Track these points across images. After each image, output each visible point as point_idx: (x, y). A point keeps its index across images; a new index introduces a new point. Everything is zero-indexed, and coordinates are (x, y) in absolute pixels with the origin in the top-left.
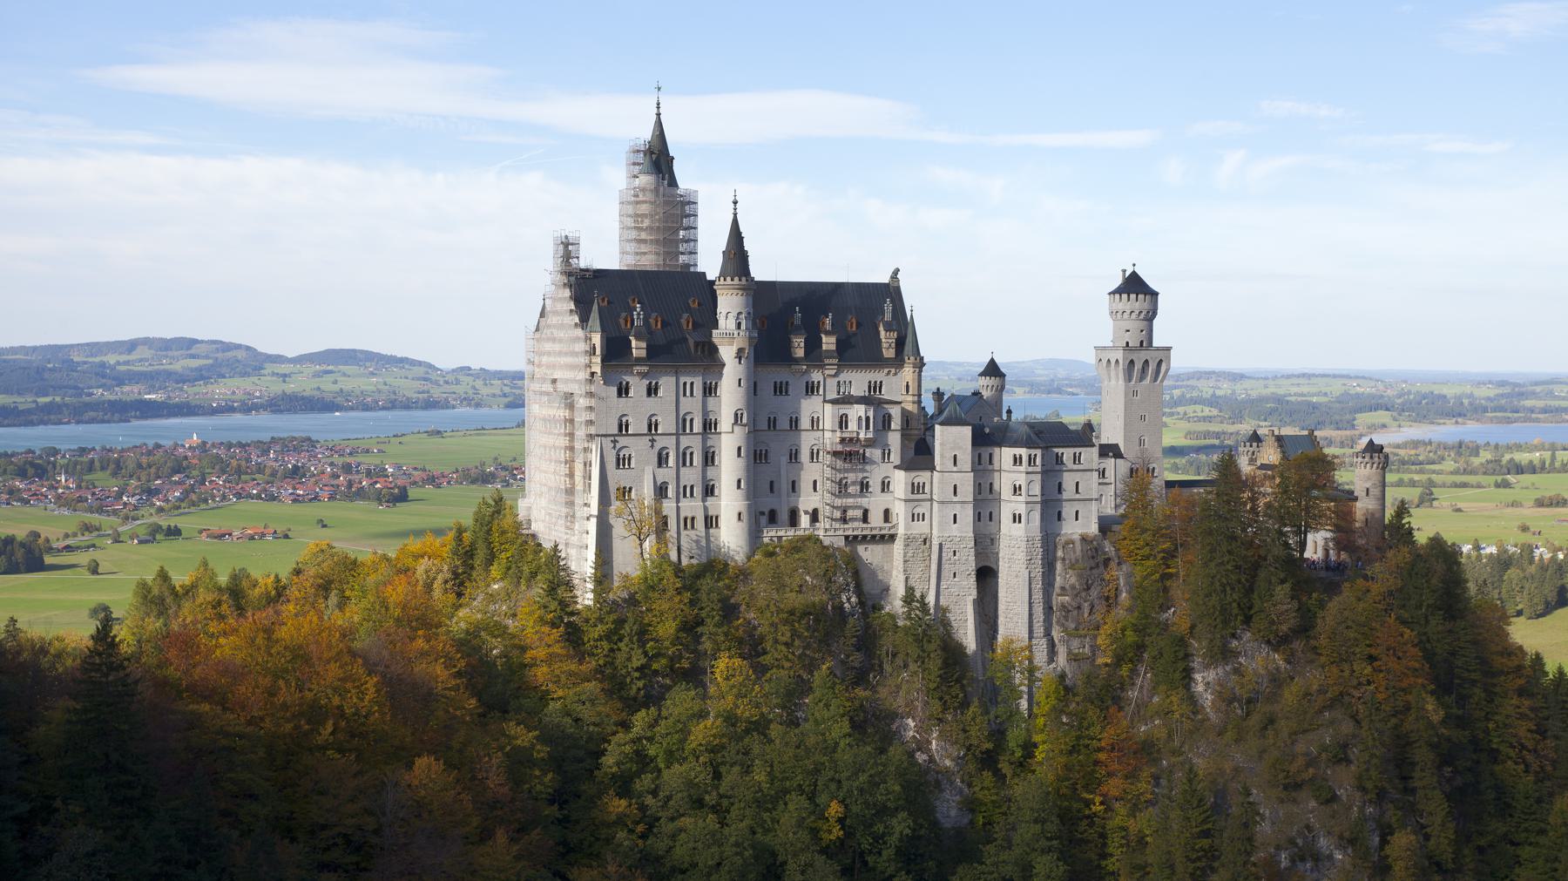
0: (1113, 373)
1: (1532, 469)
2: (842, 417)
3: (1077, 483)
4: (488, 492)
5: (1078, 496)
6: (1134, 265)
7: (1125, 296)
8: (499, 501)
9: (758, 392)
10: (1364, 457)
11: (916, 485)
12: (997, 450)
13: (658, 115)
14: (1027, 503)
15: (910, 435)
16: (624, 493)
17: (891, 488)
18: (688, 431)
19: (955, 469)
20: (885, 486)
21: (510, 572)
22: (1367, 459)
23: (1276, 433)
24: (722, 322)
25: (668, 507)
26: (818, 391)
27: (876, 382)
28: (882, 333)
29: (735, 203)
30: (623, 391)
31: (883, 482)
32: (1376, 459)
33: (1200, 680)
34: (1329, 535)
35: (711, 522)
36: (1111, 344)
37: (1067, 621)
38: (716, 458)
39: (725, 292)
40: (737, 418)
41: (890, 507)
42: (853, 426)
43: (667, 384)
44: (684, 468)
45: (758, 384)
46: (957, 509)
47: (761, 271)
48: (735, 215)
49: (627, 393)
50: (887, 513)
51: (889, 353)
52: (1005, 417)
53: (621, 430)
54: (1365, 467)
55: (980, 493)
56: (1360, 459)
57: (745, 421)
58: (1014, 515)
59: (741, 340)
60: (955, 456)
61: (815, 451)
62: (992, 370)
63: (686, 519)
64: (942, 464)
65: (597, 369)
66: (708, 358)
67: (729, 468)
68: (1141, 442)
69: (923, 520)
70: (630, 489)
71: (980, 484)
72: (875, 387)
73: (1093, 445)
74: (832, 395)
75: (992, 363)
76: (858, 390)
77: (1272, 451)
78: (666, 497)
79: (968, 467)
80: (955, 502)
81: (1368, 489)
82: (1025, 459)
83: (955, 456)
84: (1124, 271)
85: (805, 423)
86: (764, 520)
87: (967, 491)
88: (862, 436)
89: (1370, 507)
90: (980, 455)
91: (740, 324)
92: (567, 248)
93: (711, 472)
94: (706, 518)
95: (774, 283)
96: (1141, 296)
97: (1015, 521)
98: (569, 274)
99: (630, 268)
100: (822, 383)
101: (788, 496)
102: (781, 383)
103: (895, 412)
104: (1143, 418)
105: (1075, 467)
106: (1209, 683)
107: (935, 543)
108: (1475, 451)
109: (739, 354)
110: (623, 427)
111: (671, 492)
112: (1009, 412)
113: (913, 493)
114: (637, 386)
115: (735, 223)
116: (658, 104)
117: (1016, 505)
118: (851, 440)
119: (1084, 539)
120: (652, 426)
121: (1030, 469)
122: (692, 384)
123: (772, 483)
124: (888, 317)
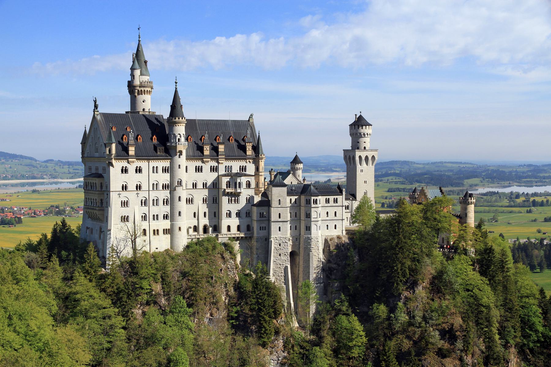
0: (352, 161)
1: (542, 204)
3: (336, 212)
4: (58, 220)
5: (336, 218)
6: (361, 112)
7: (357, 126)
8: (64, 223)
9: (188, 171)
12: (296, 197)
13: (139, 41)
16: (124, 218)
17: (250, 215)
18: (155, 189)
19: (279, 206)
25: (145, 225)
27: (243, 166)
31: (247, 212)
33: (391, 301)
37: (331, 275)
41: (250, 224)
45: (188, 167)
46: (280, 224)
48: (176, 88)
51: (250, 152)
53: (123, 189)
58: (307, 227)
60: (280, 200)
61: (215, 198)
62: (296, 160)
63: (154, 231)
68: (365, 193)
69: (265, 230)
72: (243, 169)
73: (342, 195)
75: (296, 156)
76: (236, 170)
77: (424, 197)
83: (280, 200)
84: (356, 115)
86: (191, 231)
90: (291, 199)
91: (179, 139)
94: (164, 230)
95: (195, 120)
102: (199, 166)
104: (365, 182)
107: (272, 239)
108: (518, 196)
110: (125, 188)
113: (260, 217)
114: (132, 168)
115: (176, 92)
116: (139, 36)
120: (139, 187)
122: (157, 167)
123: (195, 213)
124: (249, 136)
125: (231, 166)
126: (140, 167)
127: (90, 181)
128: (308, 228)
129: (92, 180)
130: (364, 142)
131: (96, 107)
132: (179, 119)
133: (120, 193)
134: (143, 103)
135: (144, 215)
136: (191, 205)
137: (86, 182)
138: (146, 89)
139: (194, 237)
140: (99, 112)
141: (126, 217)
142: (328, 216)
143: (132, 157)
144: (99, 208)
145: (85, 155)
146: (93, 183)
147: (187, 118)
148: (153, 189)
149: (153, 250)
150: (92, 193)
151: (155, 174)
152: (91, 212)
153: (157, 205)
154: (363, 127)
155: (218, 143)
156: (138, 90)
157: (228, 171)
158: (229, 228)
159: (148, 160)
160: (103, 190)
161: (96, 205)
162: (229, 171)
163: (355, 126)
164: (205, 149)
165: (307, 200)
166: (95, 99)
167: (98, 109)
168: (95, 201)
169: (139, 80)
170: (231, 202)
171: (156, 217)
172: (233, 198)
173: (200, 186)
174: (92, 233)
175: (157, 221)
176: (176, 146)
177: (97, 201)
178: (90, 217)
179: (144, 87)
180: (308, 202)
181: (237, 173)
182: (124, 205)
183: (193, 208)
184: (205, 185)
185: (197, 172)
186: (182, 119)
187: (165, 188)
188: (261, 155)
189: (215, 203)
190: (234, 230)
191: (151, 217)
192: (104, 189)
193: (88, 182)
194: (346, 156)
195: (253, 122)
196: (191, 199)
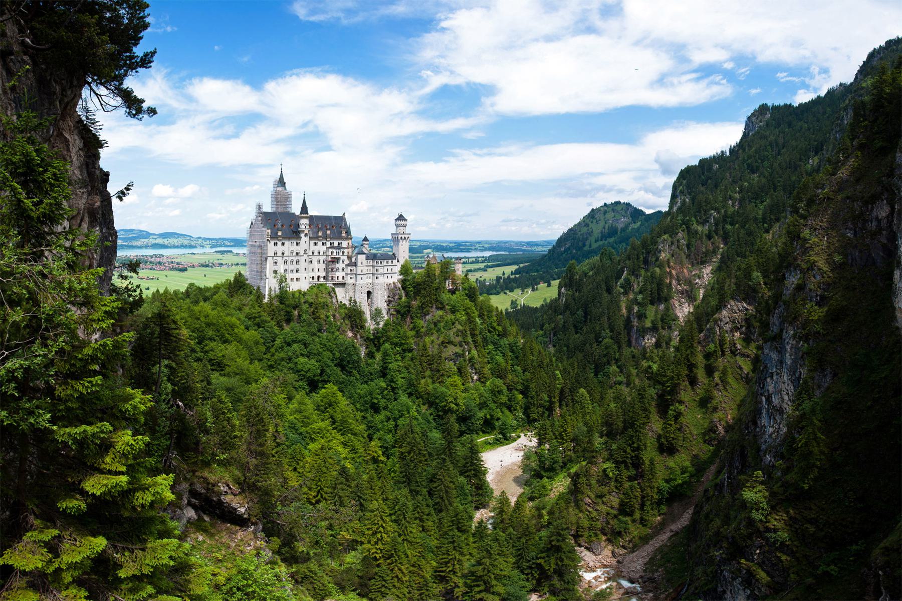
8: (240, 274)
30: (275, 244)
40: (305, 251)
42: (335, 254)
43: (287, 243)
47: (311, 212)
51: (344, 235)
59: (306, 231)
62: (366, 239)
72: (340, 244)
75: (366, 237)
76: (336, 244)
85: (322, 253)
92: (259, 207)
93: (298, 266)
109: (306, 235)
110: (275, 254)
114: (279, 243)
119: (394, 283)
120: (283, 254)
128: (377, 278)
149: (291, 290)
159: (289, 239)
171: (292, 271)
173: (316, 253)
180: (377, 263)
184: (319, 253)
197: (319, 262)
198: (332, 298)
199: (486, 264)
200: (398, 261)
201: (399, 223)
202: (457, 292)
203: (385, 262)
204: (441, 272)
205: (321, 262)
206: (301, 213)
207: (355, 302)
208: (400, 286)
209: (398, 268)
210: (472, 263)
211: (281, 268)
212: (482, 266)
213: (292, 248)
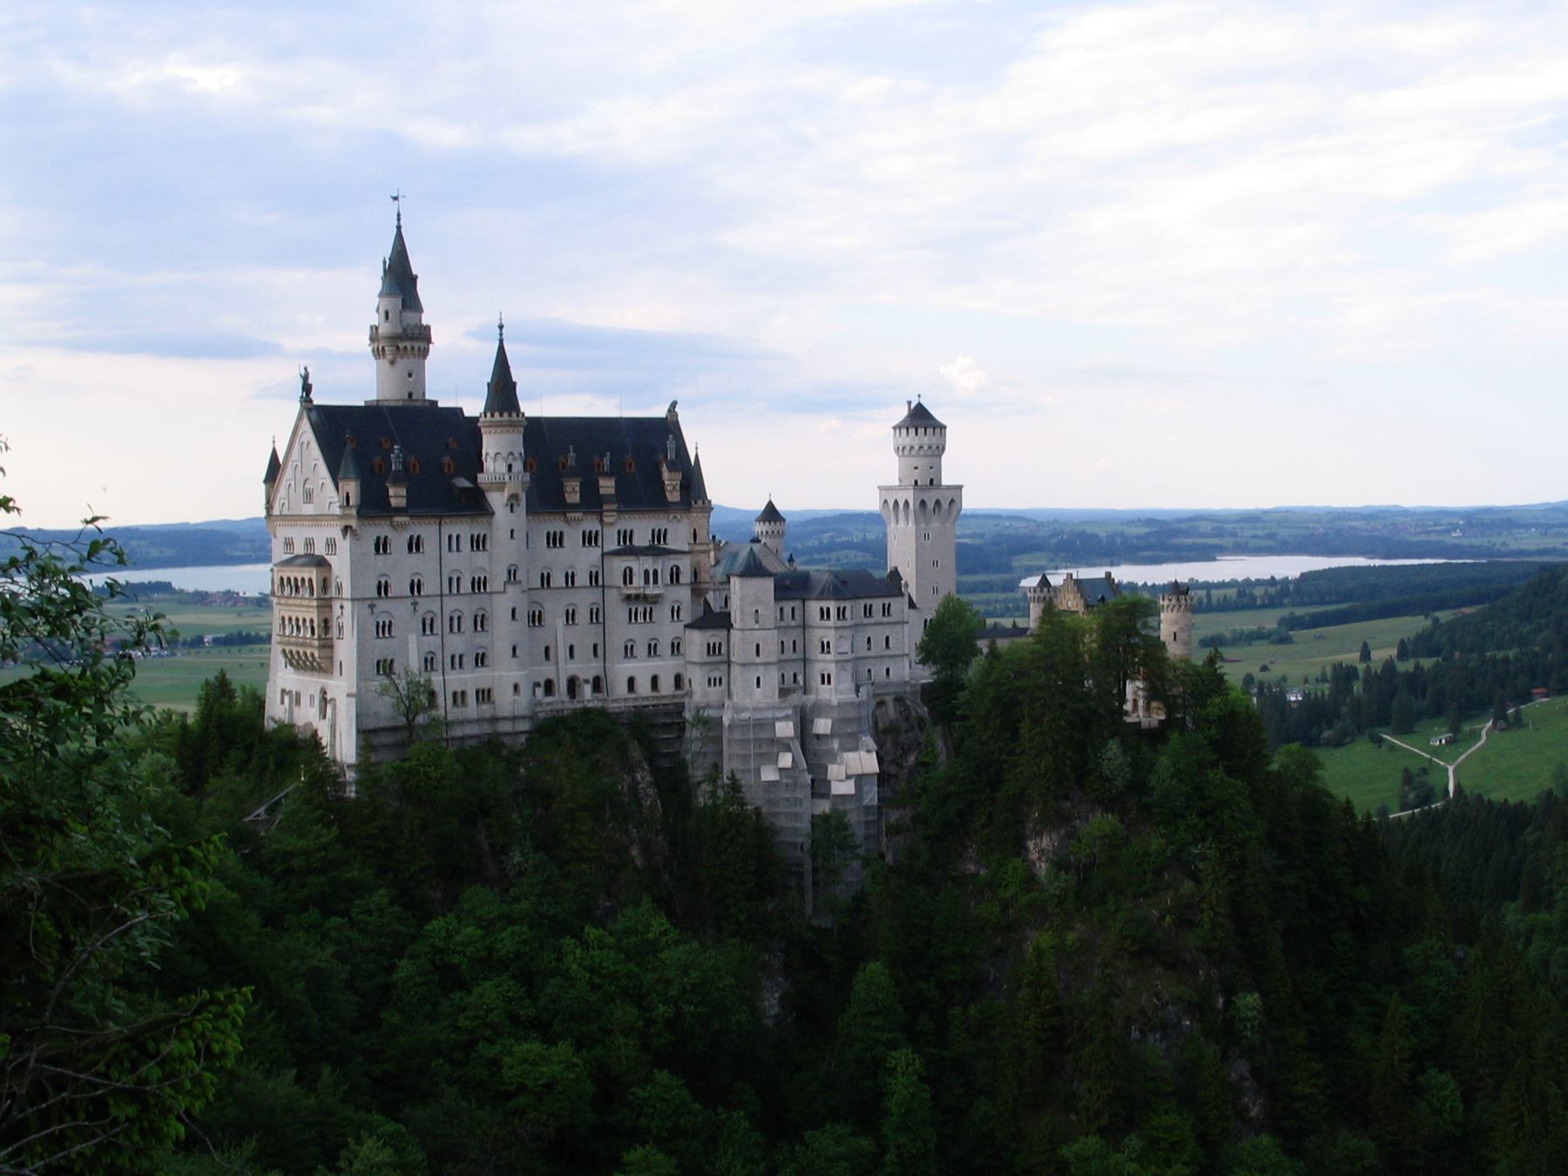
0: (901, 515)
2: (625, 571)
3: (887, 638)
6: (919, 396)
7: (912, 431)
9: (530, 545)
10: (1170, 600)
11: (712, 645)
12: (797, 604)
13: (399, 228)
14: (837, 662)
15: (700, 590)
18: (454, 591)
19: (757, 626)
20: (676, 648)
21: (253, 761)
22: (1174, 602)
23: (1075, 577)
24: (489, 465)
25: (436, 679)
26: (596, 543)
27: (659, 531)
28: (666, 475)
29: (501, 327)
30: (381, 546)
31: (673, 644)
32: (1183, 601)
34: (1140, 684)
35: (484, 695)
36: (897, 483)
38: (485, 623)
39: (490, 429)
40: (512, 574)
42: (638, 580)
44: (452, 635)
46: (761, 672)
48: (501, 341)
49: (385, 550)
50: (678, 680)
51: (673, 496)
52: (787, 564)
53: (379, 593)
54: (1172, 611)
55: (783, 652)
56: (1166, 602)
57: (517, 579)
58: (823, 676)
60: (757, 611)
62: (771, 513)
63: (455, 694)
64: (743, 621)
65: (353, 523)
66: (474, 504)
67: (503, 632)
70: (392, 661)
71: (782, 643)
72: (660, 535)
73: (902, 595)
74: (612, 545)
75: (770, 506)
76: (642, 539)
77: (1072, 597)
78: (432, 669)
79: (770, 623)
80: (761, 664)
81: (1175, 634)
82: (833, 613)
84: (909, 403)
85: (582, 579)
86: (540, 692)
87: (771, 651)
88: (648, 592)
89: (1178, 652)
90: (781, 609)
93: (480, 639)
94: (477, 692)
96: (930, 431)
97: (823, 682)
98: (309, 410)
99: (370, 404)
100: (600, 533)
101: (566, 663)
102: (555, 533)
103: (685, 564)
104: (936, 563)
105: (885, 620)
106: (1042, 850)
110: (383, 589)
111: (438, 665)
112: (791, 560)
114: (399, 541)
115: (501, 350)
116: (399, 215)
117: (824, 663)
118: (637, 596)
120: (416, 587)
121: (840, 623)
122: (458, 537)
123: (547, 649)
124: (671, 455)
125: (631, 532)
126: (418, 537)
127: (295, 574)
129: (299, 572)
130: (931, 468)
131: (307, 388)
132: (510, 415)
133: (375, 602)
134: (411, 379)
135: (429, 658)
136: (538, 631)
137: (282, 579)
138: (416, 345)
139: (549, 708)
140: (316, 402)
141: (389, 662)
142: (869, 649)
143: (399, 511)
144: (322, 642)
145: (276, 511)
146: (303, 580)
147: (526, 415)
148: (450, 591)
150: (303, 606)
151: (455, 553)
152: (298, 653)
153: (459, 629)
154: (928, 430)
155: (606, 475)
156: (398, 348)
157: (625, 542)
158: (631, 681)
159: (440, 518)
160: (326, 596)
161: (313, 633)
162: (628, 543)
163: (908, 429)
164: (569, 489)
165: (822, 609)
166: (303, 372)
167: (311, 396)
168: (308, 624)
169: (401, 322)
170: (636, 619)
171: (457, 662)
172: (641, 610)
173: (558, 580)
174: (298, 702)
175: (462, 670)
176: (505, 483)
177: (315, 625)
178: (291, 665)
179: (412, 339)
181: (647, 548)
182: (383, 633)
183: (543, 636)
184: (570, 578)
185: (551, 545)
186: (518, 415)
187: (479, 589)
188: (704, 503)
189: (594, 621)
190: (644, 688)
191: (448, 661)
192: (333, 592)
193: (289, 579)
194: (886, 501)
195: (677, 422)
196: (537, 613)
197: (570, 617)
198: (631, 769)
199: (1285, 612)
200: (912, 605)
201: (910, 439)
202: (1175, 736)
203: (854, 608)
204: (1104, 647)
205: (583, 616)
206: (490, 407)
207: (735, 786)
208: (924, 710)
209: (910, 636)
210: (1225, 607)
211: (411, 650)
212: (1269, 620)
213: (453, 561)
